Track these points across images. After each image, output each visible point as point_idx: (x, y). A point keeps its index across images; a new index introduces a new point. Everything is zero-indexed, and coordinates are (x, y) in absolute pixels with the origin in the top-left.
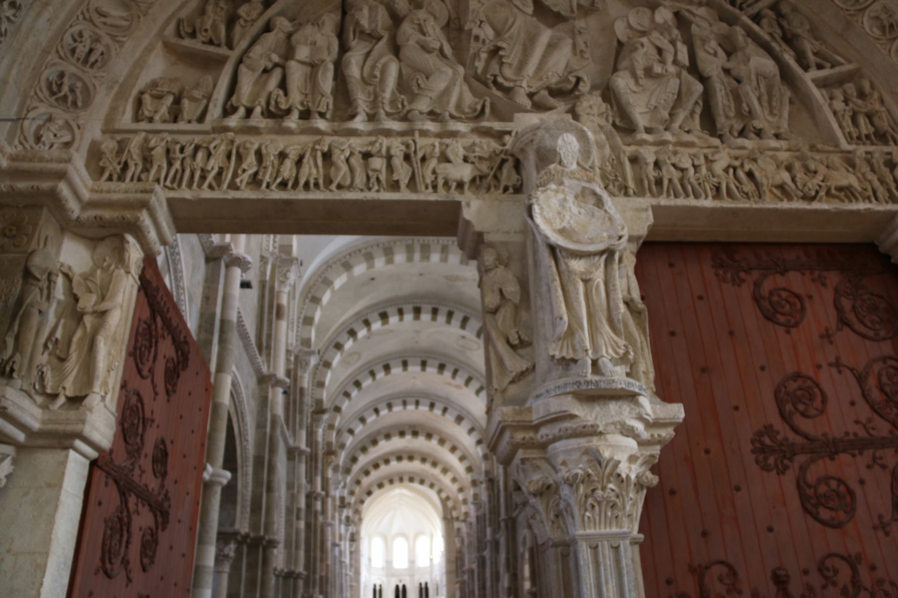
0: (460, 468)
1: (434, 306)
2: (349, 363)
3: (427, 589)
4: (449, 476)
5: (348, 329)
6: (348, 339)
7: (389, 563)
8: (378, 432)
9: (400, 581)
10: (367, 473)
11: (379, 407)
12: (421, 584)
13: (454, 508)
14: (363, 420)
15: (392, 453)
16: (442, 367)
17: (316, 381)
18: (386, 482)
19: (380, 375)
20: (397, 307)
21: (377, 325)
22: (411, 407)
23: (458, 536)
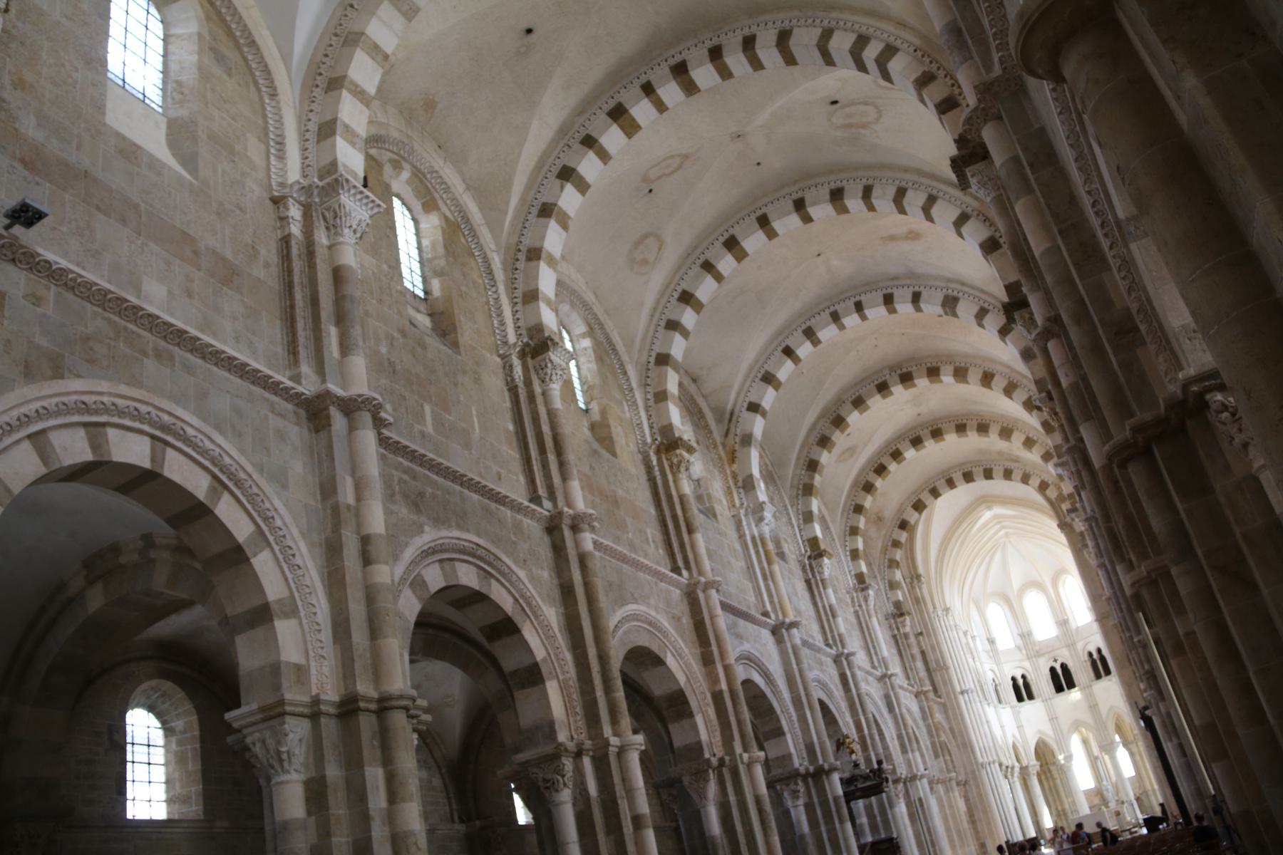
0: (1012, 408)
1: (709, 44)
2: (644, 262)
3: (1103, 659)
4: (1018, 438)
5: (556, 170)
6: (562, 188)
7: (1026, 636)
8: (839, 401)
9: (1056, 661)
10: (868, 488)
11: (790, 342)
12: (1090, 654)
14: (769, 379)
15: (899, 437)
16: (837, 196)
17: (519, 293)
19: (726, 264)
20: (637, 83)
21: (612, 138)
22: (851, 320)
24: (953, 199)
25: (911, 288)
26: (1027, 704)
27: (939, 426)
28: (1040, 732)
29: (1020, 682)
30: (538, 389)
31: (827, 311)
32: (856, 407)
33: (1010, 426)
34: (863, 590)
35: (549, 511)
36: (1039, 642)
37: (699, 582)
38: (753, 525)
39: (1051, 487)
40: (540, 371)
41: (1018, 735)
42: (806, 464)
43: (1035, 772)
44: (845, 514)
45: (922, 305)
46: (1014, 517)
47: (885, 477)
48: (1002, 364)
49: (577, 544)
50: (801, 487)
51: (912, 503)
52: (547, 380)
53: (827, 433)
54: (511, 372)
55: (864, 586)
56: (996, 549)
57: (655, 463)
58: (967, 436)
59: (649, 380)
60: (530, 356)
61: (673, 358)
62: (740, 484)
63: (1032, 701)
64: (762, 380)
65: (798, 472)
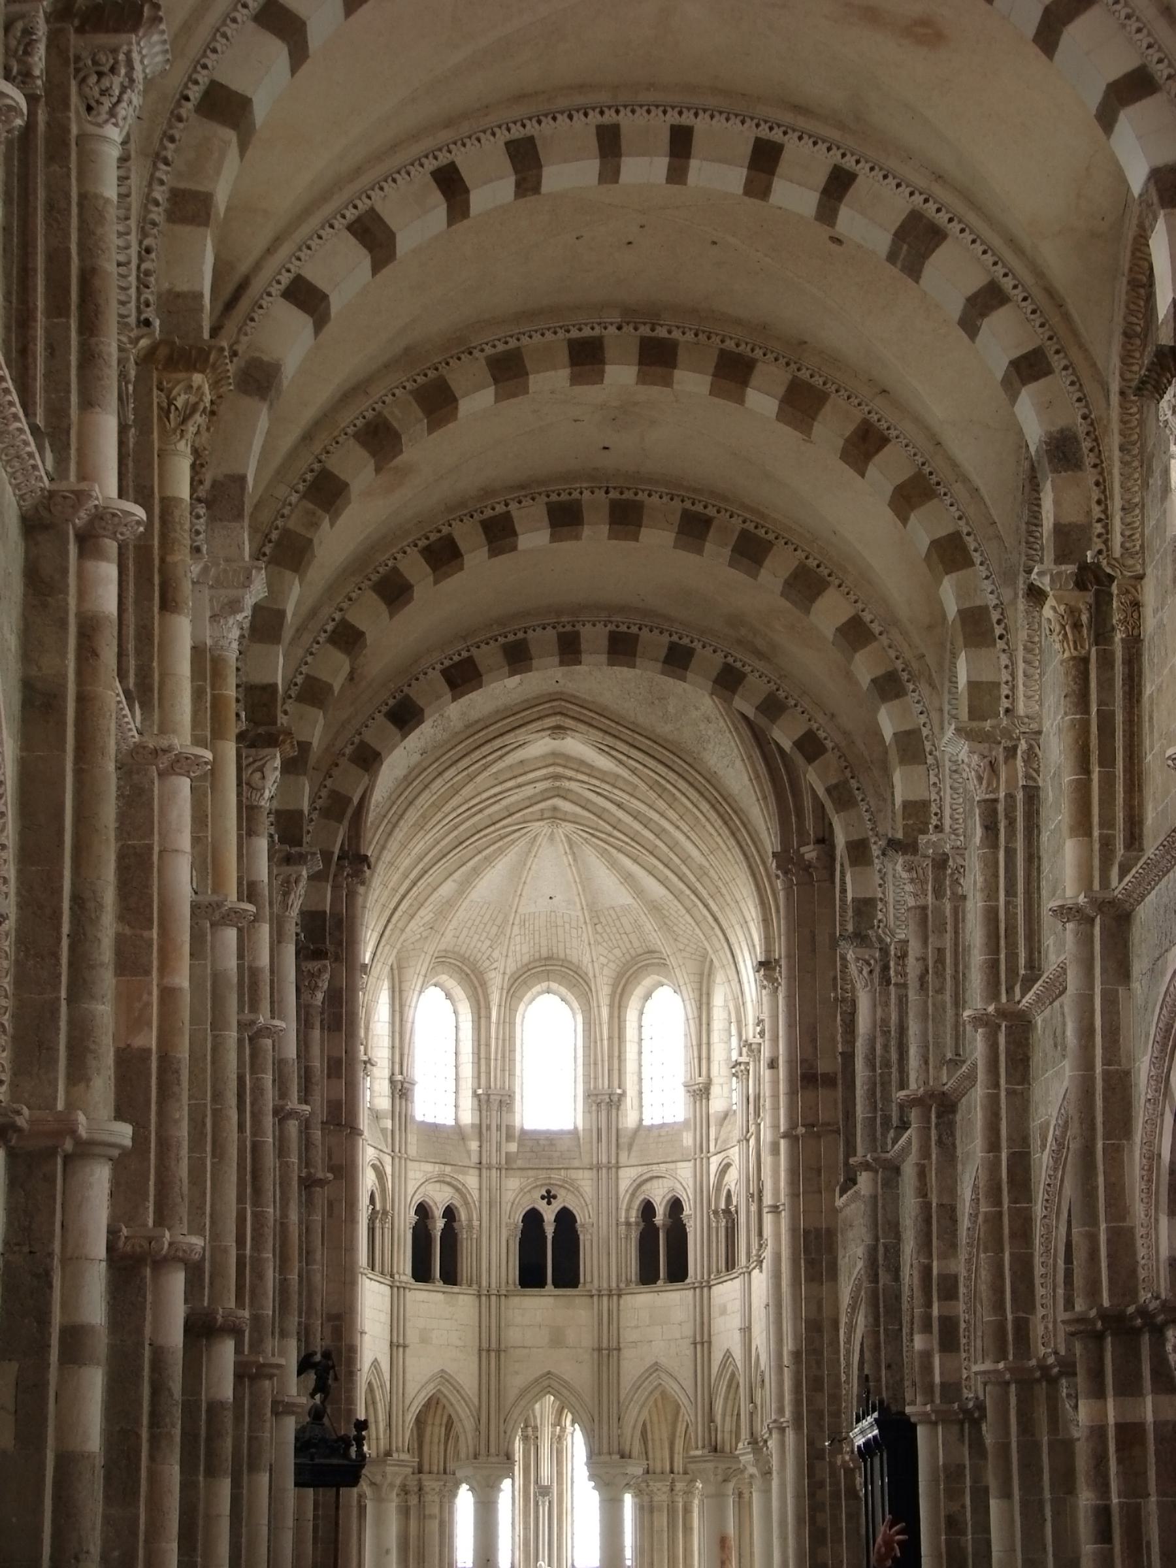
9: (549, 1197)
11: (464, 160)
12: (648, 1209)
13: (843, 797)
15: (525, 489)
18: (488, 656)
23: (860, 938)
24: (1133, 25)
25: (835, 156)
26: (439, 1284)
27: (641, 496)
28: (444, 1376)
29: (440, 1224)
30: (74, 130)
31: (595, 118)
32: (496, 381)
33: (824, 571)
34: (288, 860)
35: (52, 480)
36: (523, 1132)
37: (164, 751)
38: (208, 614)
39: (830, 757)
40: (94, 78)
41: (385, 1366)
42: (309, 477)
43: (398, 1482)
44: (307, 638)
45: (845, 213)
46: (603, 776)
47: (447, 575)
48: (917, 420)
49: (82, 595)
50: (275, 535)
51: (447, 663)
52: (107, 104)
53: (395, 416)
54: (26, 53)
55: (294, 850)
56: (513, 841)
57: (131, 388)
58: (700, 551)
59: (171, 146)
60: (76, 22)
61: (251, 112)
62: (202, 492)
63: (456, 1289)
64: (349, 228)
65: (282, 491)
